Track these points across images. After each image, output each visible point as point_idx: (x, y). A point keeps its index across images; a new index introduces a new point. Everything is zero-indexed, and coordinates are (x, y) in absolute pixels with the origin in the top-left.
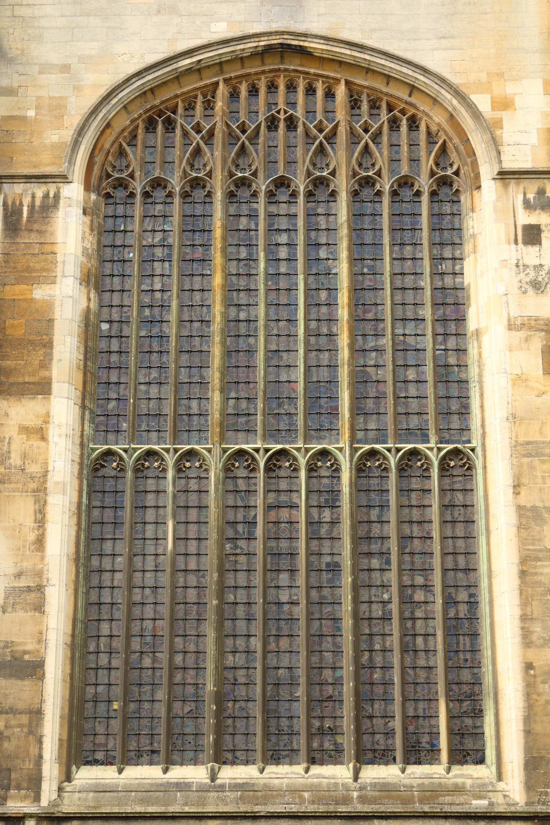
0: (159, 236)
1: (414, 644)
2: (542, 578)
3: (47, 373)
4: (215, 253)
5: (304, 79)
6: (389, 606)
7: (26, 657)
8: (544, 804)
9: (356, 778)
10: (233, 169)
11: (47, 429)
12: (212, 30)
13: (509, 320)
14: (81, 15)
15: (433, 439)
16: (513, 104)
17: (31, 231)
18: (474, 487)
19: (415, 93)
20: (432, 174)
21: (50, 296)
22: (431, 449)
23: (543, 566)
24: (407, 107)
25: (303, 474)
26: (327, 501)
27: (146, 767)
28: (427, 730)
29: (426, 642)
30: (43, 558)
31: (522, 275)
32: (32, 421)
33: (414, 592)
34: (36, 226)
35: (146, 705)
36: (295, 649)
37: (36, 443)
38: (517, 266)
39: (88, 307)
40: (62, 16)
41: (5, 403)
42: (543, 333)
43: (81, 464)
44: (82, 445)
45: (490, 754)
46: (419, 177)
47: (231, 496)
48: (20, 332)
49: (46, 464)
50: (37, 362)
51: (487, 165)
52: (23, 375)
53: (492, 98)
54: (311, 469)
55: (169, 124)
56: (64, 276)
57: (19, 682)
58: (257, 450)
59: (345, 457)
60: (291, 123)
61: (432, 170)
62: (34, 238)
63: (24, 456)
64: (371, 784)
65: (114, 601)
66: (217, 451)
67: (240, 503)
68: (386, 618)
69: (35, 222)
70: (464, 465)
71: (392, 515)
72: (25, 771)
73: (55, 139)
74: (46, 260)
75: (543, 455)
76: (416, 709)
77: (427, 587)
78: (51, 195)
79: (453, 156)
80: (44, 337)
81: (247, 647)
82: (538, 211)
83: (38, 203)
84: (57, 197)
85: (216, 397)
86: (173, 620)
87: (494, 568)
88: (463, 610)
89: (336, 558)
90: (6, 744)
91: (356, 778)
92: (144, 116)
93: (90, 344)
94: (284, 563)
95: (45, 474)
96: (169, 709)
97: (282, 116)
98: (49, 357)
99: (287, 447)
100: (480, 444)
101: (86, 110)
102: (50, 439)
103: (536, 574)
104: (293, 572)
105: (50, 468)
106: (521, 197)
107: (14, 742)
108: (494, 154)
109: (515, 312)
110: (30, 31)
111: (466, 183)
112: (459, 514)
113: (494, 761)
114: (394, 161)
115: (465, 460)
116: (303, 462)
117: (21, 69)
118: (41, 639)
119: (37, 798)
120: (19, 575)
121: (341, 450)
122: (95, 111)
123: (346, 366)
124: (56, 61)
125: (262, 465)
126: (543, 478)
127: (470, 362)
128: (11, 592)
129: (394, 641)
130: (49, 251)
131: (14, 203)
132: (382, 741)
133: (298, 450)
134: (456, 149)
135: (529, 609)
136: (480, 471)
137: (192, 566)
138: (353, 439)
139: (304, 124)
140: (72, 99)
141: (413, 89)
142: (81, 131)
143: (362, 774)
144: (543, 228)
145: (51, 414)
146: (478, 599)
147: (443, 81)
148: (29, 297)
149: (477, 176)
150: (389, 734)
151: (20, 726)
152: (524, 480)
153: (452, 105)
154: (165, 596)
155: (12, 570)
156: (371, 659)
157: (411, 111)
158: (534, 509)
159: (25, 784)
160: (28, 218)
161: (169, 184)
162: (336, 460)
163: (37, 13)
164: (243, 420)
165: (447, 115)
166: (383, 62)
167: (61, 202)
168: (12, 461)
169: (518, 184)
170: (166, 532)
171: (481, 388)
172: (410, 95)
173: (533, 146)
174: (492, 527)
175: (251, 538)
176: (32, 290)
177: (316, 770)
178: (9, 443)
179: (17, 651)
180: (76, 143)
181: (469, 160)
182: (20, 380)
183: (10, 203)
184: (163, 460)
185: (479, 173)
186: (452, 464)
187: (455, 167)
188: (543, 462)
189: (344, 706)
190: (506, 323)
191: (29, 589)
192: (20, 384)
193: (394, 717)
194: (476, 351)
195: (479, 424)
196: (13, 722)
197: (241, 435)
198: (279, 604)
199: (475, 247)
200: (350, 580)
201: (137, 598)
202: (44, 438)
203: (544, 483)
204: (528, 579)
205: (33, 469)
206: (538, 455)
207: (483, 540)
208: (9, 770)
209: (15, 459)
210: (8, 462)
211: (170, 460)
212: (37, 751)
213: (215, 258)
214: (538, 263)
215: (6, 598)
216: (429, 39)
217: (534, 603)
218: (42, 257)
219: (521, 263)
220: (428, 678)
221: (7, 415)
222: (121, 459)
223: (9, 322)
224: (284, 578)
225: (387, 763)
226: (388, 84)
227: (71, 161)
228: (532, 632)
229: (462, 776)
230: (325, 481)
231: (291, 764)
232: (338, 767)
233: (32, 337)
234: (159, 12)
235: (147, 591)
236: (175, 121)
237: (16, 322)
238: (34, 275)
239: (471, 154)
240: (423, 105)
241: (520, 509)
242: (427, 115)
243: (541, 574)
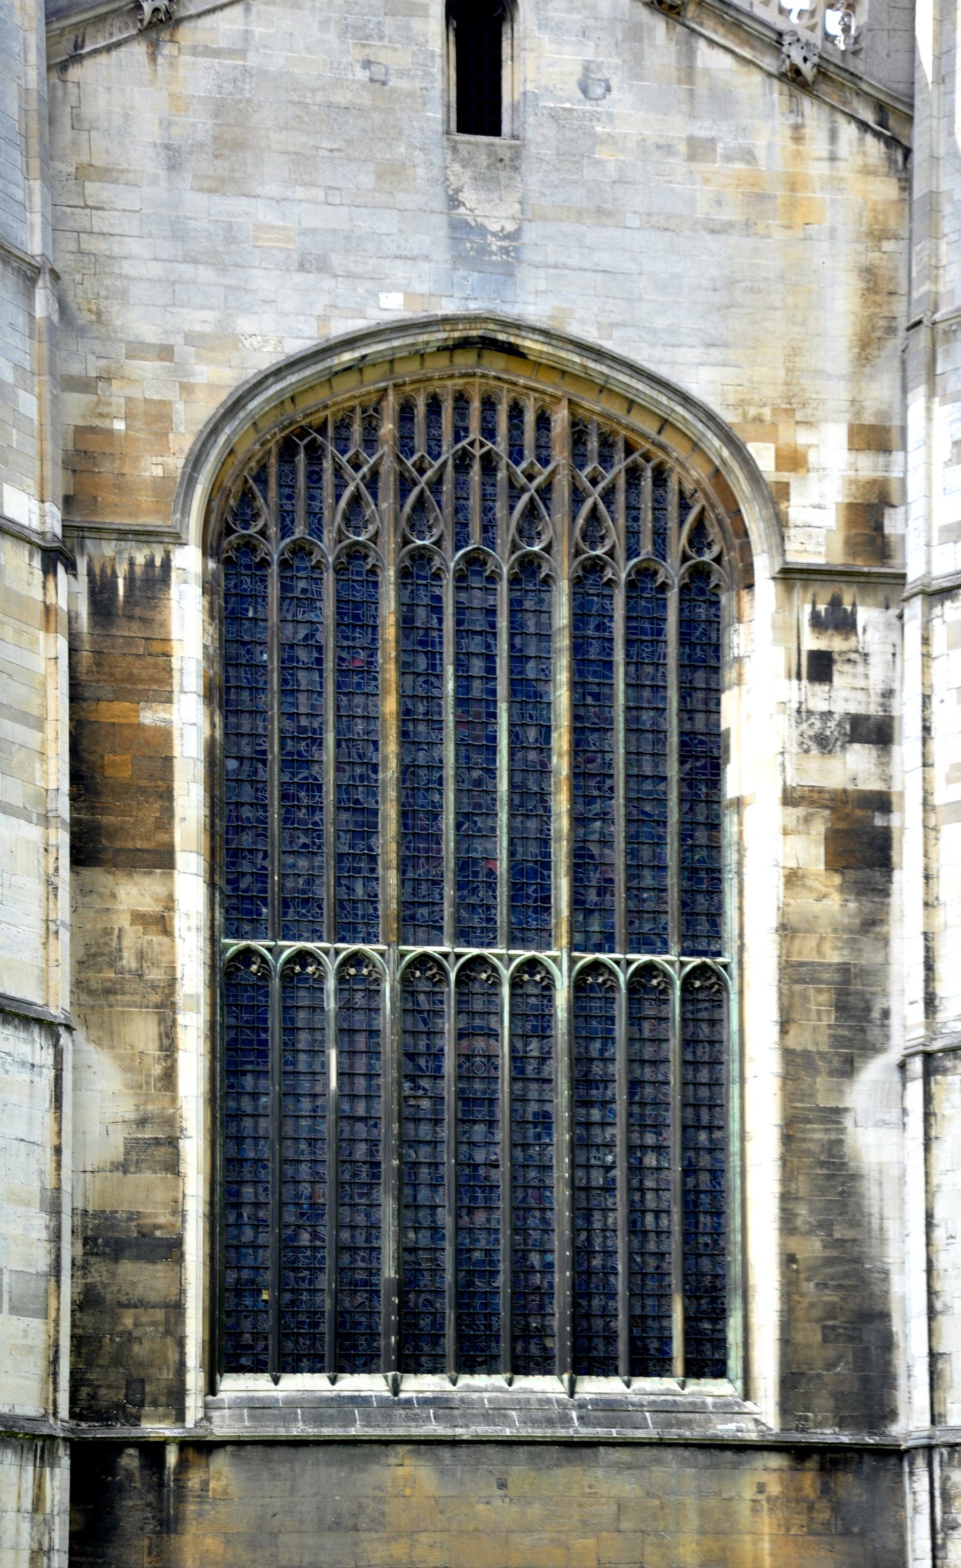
0: (302, 632)
1: (643, 1224)
2: (811, 1146)
3: (166, 838)
4: (385, 662)
5: (509, 390)
6: (613, 1173)
7: (158, 1233)
8: (803, 1431)
9: (572, 1393)
10: (408, 532)
11: (172, 919)
12: (383, 306)
13: (785, 790)
14: (184, 261)
15: (675, 948)
16: (806, 462)
17: (131, 618)
18: (724, 1017)
19: (668, 431)
20: (685, 558)
21: (165, 720)
22: (671, 963)
23: (814, 1130)
24: (653, 449)
25: (506, 990)
26: (534, 1028)
27: (307, 1376)
28: (656, 1334)
29: (657, 1218)
30: (174, 1100)
31: (804, 726)
32: (149, 906)
33: (644, 1154)
34: (138, 612)
35: (305, 1297)
36: (493, 1224)
37: (157, 939)
38: (799, 711)
39: (212, 736)
40: (155, 259)
41: (110, 878)
42: (828, 812)
43: (213, 967)
44: (213, 940)
45: (734, 1364)
46: (664, 559)
47: (409, 1018)
48: (125, 774)
49: (173, 969)
50: (152, 820)
51: (765, 556)
52: (133, 839)
53: (777, 450)
54: (516, 984)
55: (315, 453)
56: (182, 691)
57: (150, 1267)
58: (445, 955)
59: (560, 970)
60: (489, 464)
61: (684, 552)
62: (135, 630)
63: (141, 956)
64: (592, 1402)
65: (259, 1155)
66: (392, 955)
67: (421, 1027)
68: (609, 1188)
69: (137, 604)
70: (712, 985)
71: (620, 1051)
72: (162, 1383)
73: (158, 471)
74: (155, 666)
75: (820, 982)
76: (643, 1307)
77: (659, 1149)
78: (158, 562)
79: (713, 532)
80: (160, 783)
81: (434, 1221)
82: (830, 632)
83: (138, 570)
84: (166, 564)
85: (393, 878)
86: (340, 1184)
87: (748, 1128)
88: (705, 1178)
89: (547, 1107)
90: (136, 1348)
91: (572, 1393)
92: (278, 437)
93: (217, 792)
94: (480, 1112)
95: (172, 983)
96: (337, 1302)
97: (477, 452)
98: (168, 812)
99: (486, 951)
100: (736, 960)
101: (200, 427)
102: (177, 934)
103: (804, 1140)
104: (491, 1124)
105: (179, 975)
106: (808, 608)
107: (147, 1345)
108: (776, 540)
110: (107, 282)
111: (731, 576)
112: (703, 1053)
113: (740, 1374)
114: (633, 534)
115: (714, 980)
116: (506, 974)
117: (98, 346)
118: (178, 1211)
119: (180, 1417)
120: (142, 1122)
121: (555, 959)
122: (214, 430)
123: (565, 843)
124: (152, 339)
125: (453, 976)
126: (819, 1012)
127: (725, 842)
128: (132, 1145)
129: (619, 1217)
130: (159, 651)
131: (103, 571)
132: (601, 1347)
133: (499, 957)
134: (720, 523)
135: (794, 1186)
136: (734, 997)
137: (361, 1111)
138: (573, 947)
139: (508, 466)
140: (179, 407)
141: (664, 424)
142: (196, 462)
143: (578, 1388)
144: (836, 657)
145: (176, 897)
146: (725, 1166)
147: (710, 418)
148: (133, 720)
149: (749, 569)
150: (611, 1338)
151: (154, 1324)
152: (795, 1015)
153: (721, 457)
154: (328, 1154)
155: (132, 1115)
156: (589, 1239)
157: (660, 455)
158: (806, 1054)
159: (163, 1399)
160: (125, 596)
161: (316, 550)
162: (548, 972)
163: (116, 249)
164: (424, 911)
165: (710, 470)
166: (626, 379)
167: (173, 574)
168: (124, 962)
169: (805, 588)
170: (325, 1065)
171: (741, 882)
172: (659, 432)
173: (829, 530)
174: (748, 1073)
175: (437, 1076)
176: (137, 711)
177: (522, 1382)
178: (119, 937)
179: (145, 1226)
180: (190, 482)
181: (737, 542)
182: (130, 845)
183: (97, 570)
184: (320, 963)
185: (751, 565)
186: (697, 984)
187: (716, 549)
188: (819, 991)
189: (555, 1301)
190: (779, 794)
191: (157, 1142)
192: (129, 851)
193: (616, 1316)
194: (735, 829)
195: (736, 932)
196: (144, 1319)
197: (421, 933)
198: (476, 1167)
199: (740, 675)
200: (567, 1137)
201: (290, 1154)
202: (167, 931)
203: (820, 1020)
204: (794, 1146)
205: (155, 975)
206: (815, 981)
207: (735, 1090)
208: (142, 1381)
209: (129, 960)
210: (119, 964)
211: (331, 966)
212: (176, 1357)
213: (384, 671)
214: (824, 707)
215: (127, 1153)
216: (692, 347)
217: (801, 1178)
218: (150, 660)
219: (804, 708)
220: (658, 1267)
221: (114, 896)
222: (264, 960)
223: (109, 758)
224: (479, 1131)
225: (606, 1374)
226: (629, 411)
227: (185, 512)
228: (796, 1215)
229: (701, 1394)
230: (533, 1001)
231: (490, 1372)
232: (548, 1377)
233: (143, 783)
234: (302, 267)
235: (303, 1146)
236: (321, 448)
237: (118, 759)
238: (140, 687)
239: (741, 532)
240: (678, 449)
241: (788, 1055)
242: (682, 465)
243: (811, 1140)
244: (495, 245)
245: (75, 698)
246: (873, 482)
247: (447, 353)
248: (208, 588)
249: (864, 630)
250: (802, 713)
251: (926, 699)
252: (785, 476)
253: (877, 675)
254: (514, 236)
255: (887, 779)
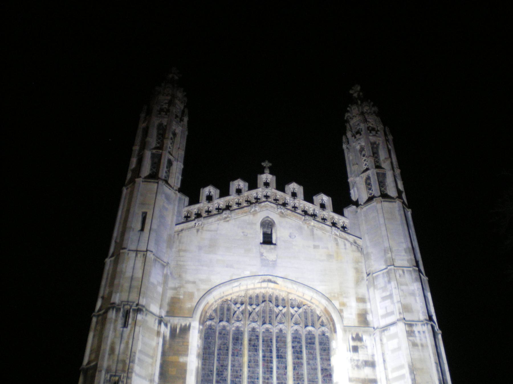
38: (351, 360)
39: (198, 366)
73: (190, 306)
109: (351, 376)
144: (359, 347)
219: (352, 359)
223: (170, 369)
244: (271, 263)
245: (164, 354)
246: (363, 309)
247: (260, 283)
248: (200, 331)
249: (365, 341)
250: (352, 360)
251: (383, 354)
252: (342, 308)
253: (370, 351)
254: (275, 261)
255: (376, 375)
